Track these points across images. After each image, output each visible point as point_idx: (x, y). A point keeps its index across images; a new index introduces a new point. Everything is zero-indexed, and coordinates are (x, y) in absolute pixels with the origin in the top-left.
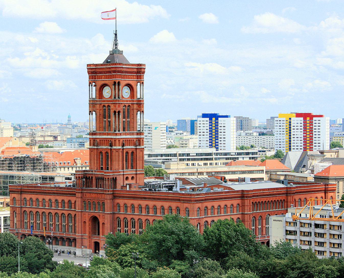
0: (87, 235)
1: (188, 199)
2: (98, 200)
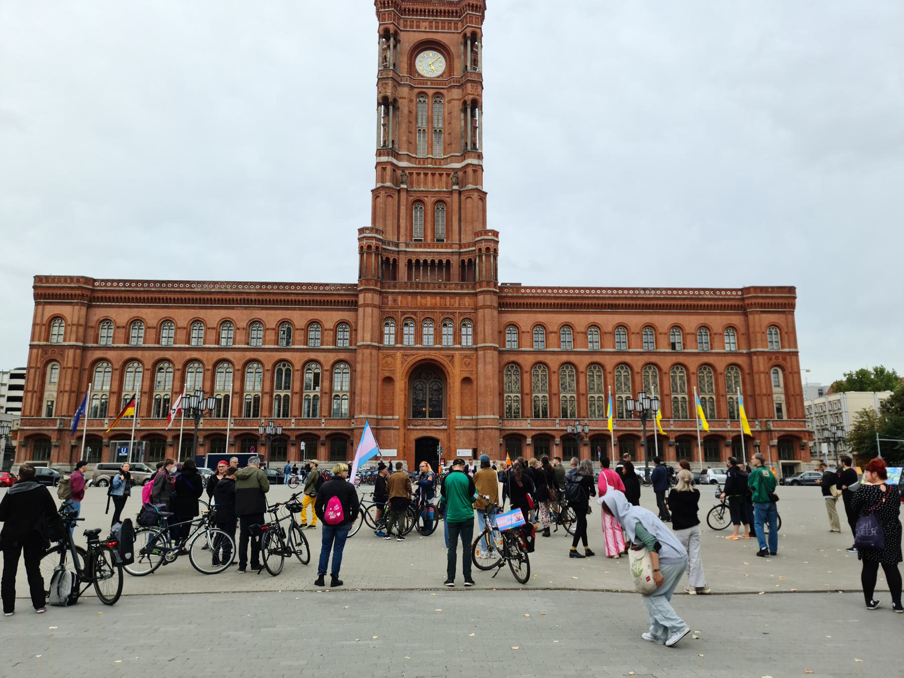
0: (397, 417)
1: (780, 301)
2: (443, 313)
